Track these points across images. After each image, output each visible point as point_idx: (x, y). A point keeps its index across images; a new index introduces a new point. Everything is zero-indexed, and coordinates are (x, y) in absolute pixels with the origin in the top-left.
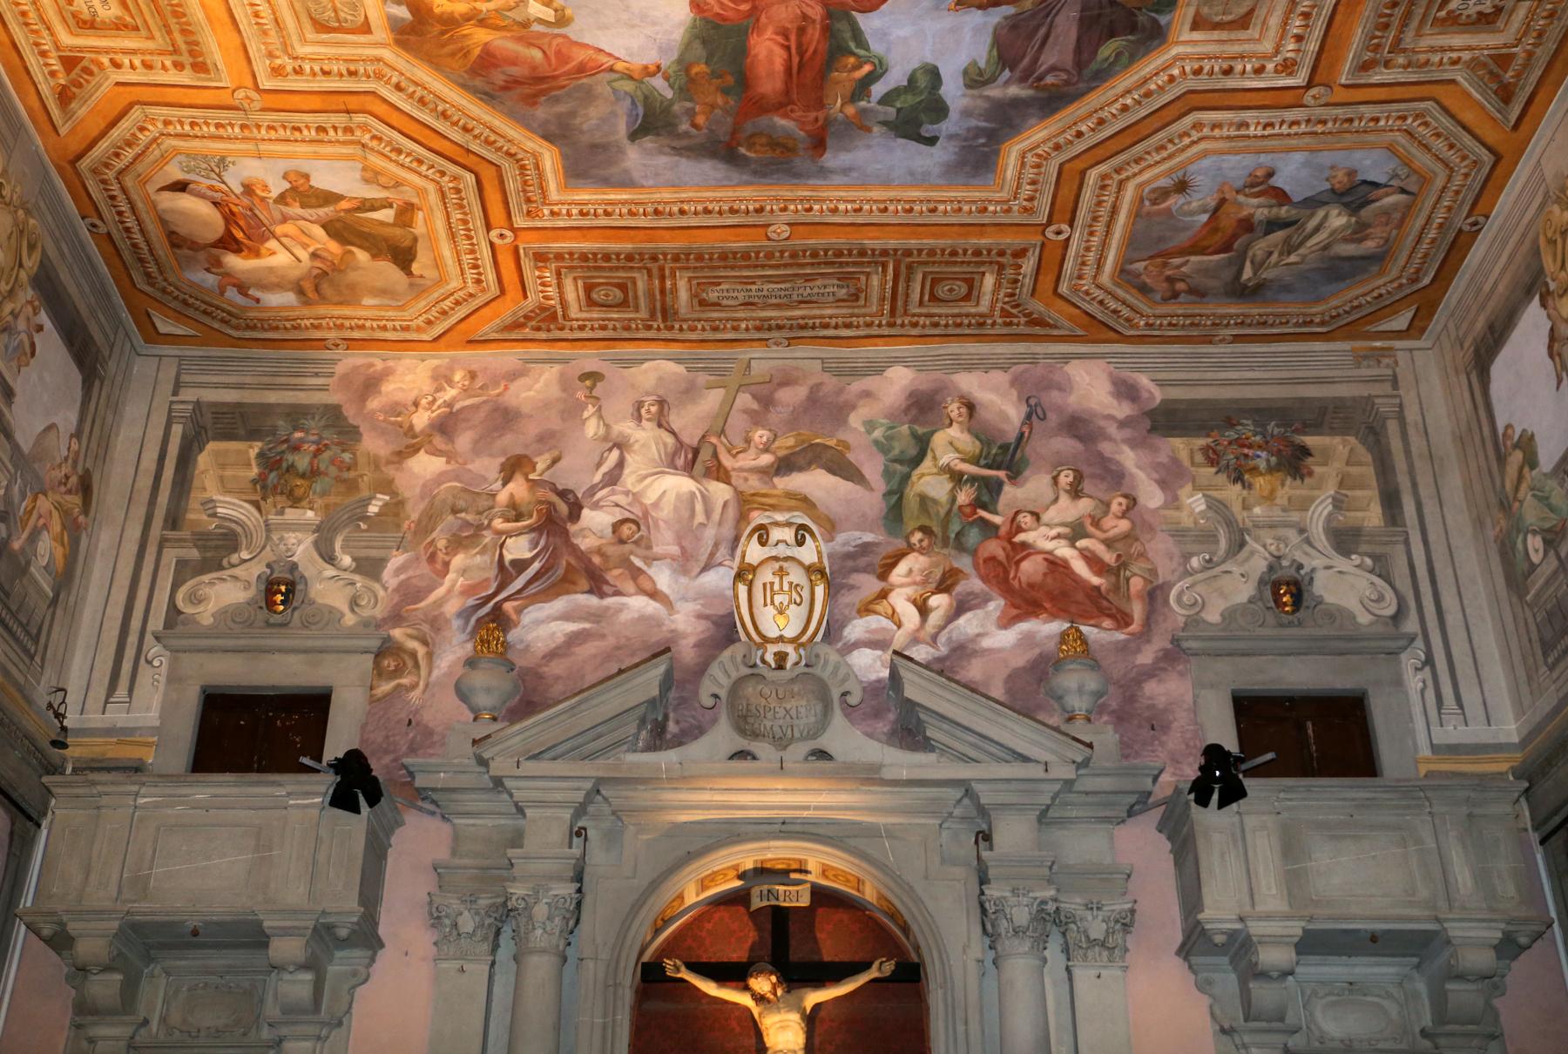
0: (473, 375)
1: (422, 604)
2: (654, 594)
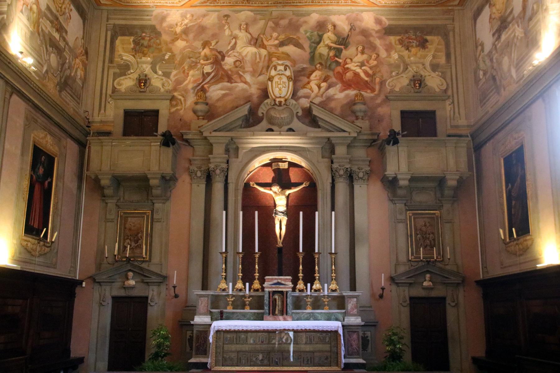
1: (182, 86)
2: (246, 83)
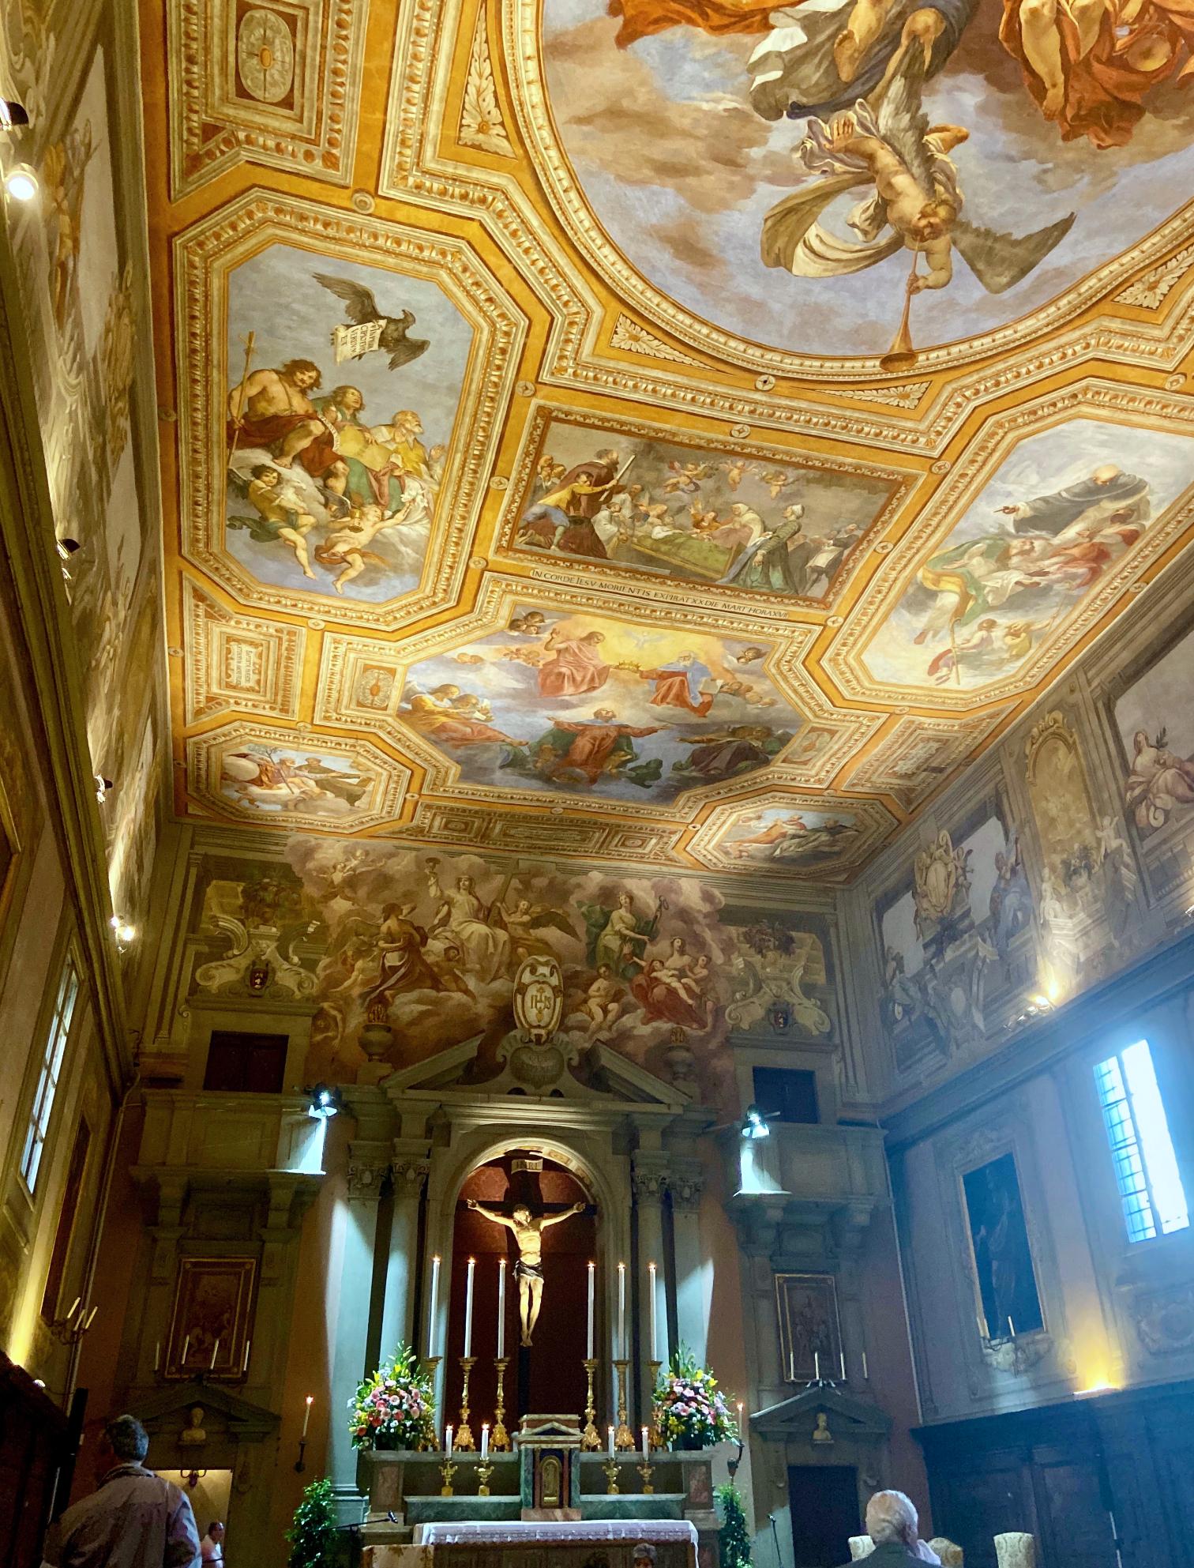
0: (367, 854)
2: (466, 992)
